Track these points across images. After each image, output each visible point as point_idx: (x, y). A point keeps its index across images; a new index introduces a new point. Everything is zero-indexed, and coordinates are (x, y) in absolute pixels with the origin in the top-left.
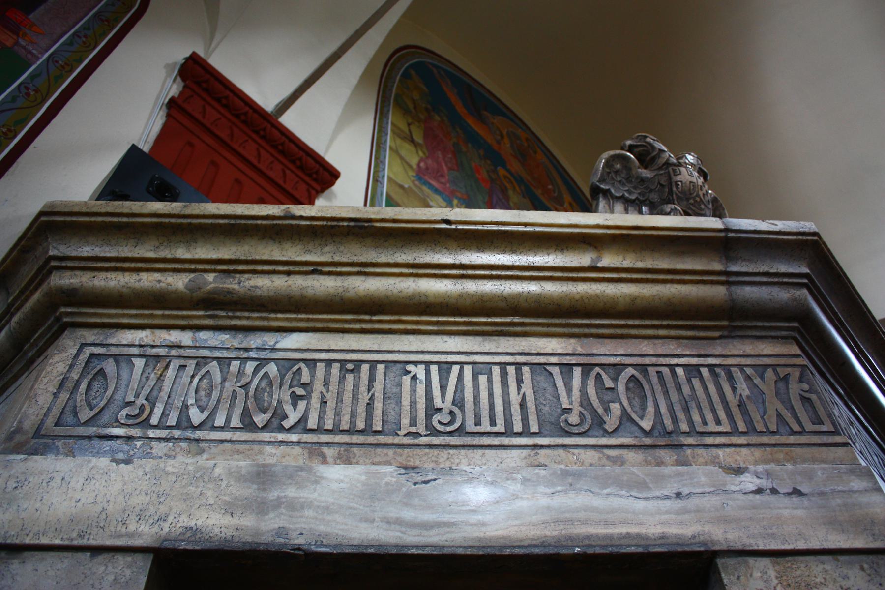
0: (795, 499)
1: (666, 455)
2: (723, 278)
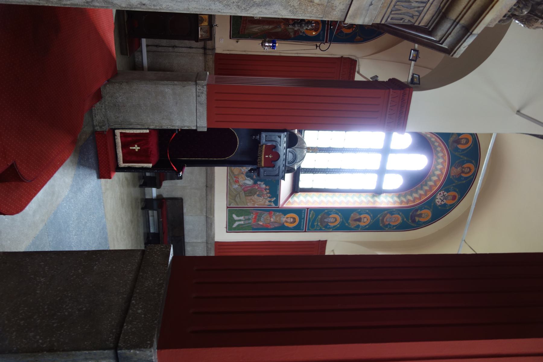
0: (369, 3)
2: (457, 21)
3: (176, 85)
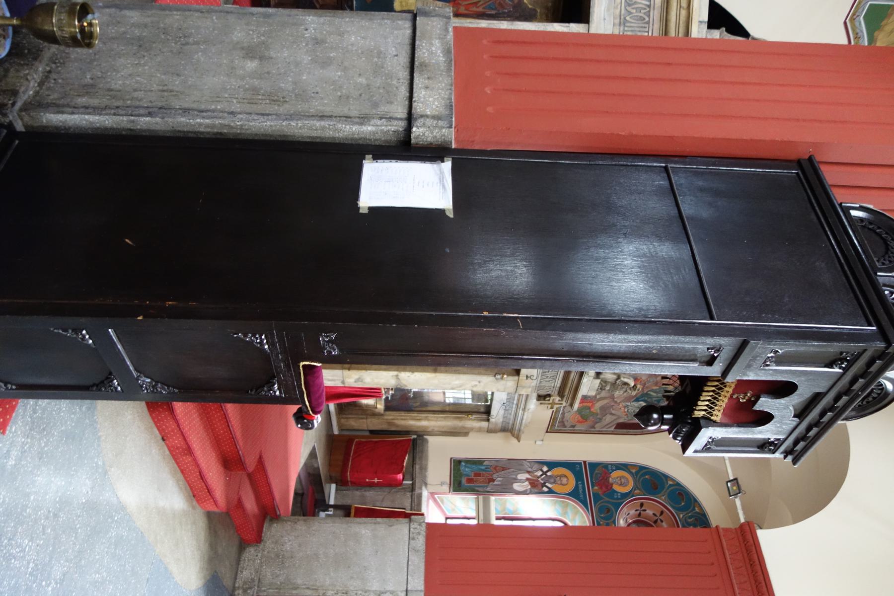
1: (617, 21)
3: (379, 523)
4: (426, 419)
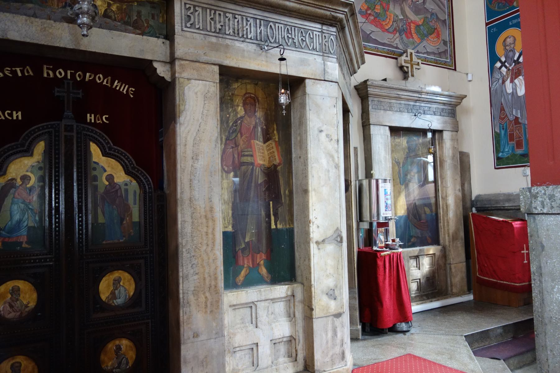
4: (445, 199)
